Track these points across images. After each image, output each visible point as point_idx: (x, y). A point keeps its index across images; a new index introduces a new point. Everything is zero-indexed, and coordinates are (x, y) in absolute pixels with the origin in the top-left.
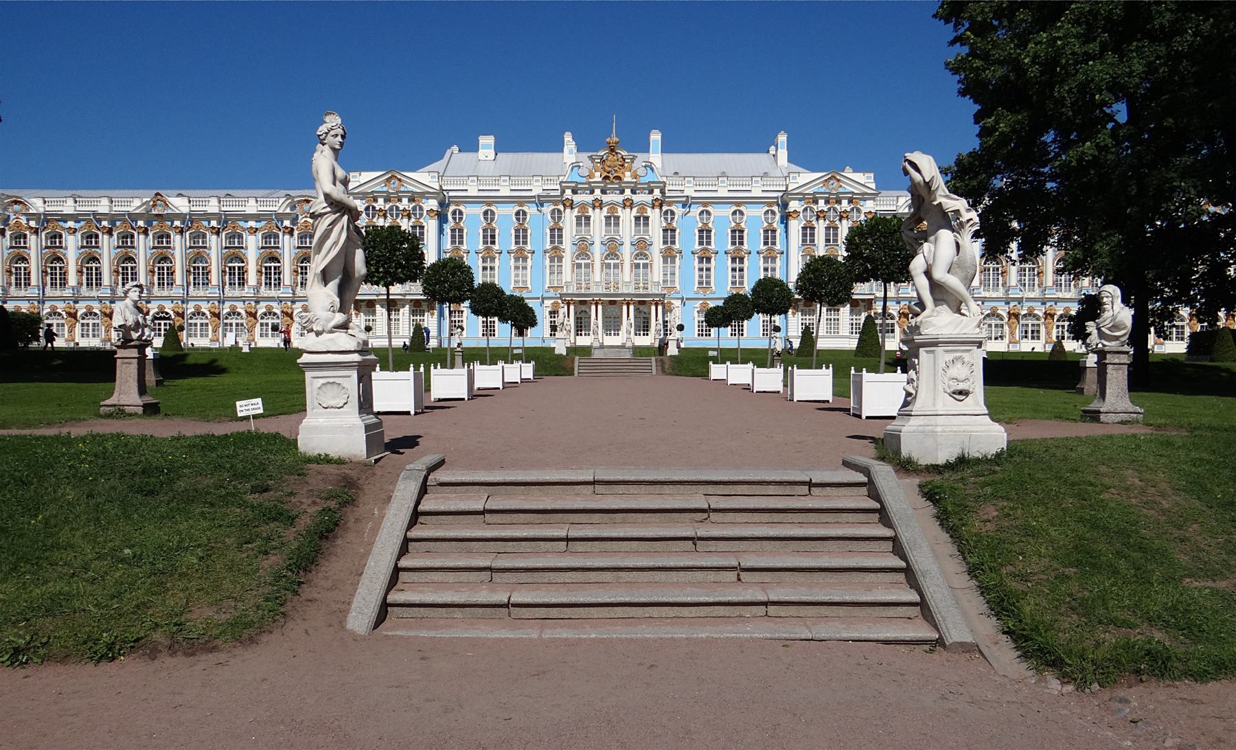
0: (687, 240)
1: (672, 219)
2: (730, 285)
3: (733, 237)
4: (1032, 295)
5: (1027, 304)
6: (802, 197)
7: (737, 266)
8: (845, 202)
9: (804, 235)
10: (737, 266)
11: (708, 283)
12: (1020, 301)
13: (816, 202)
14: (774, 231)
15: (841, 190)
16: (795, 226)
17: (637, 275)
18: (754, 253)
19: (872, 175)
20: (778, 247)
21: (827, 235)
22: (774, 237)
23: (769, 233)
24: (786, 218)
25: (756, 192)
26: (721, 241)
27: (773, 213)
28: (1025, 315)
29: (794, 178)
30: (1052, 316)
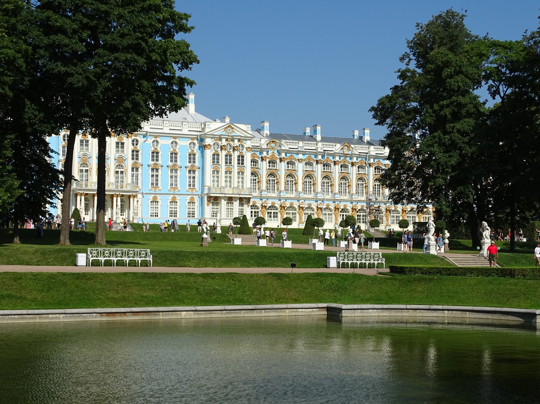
0: (145, 158)
1: (137, 144)
2: (188, 187)
3: (172, 157)
4: (328, 197)
5: (326, 203)
6: (213, 137)
7: (155, 173)
8: (236, 141)
9: (214, 159)
10: (174, 174)
11: (157, 184)
12: (323, 200)
13: (220, 139)
14: (194, 155)
15: (233, 134)
16: (209, 153)
17: (117, 178)
18: (183, 168)
19: (250, 126)
20: (198, 164)
21: (226, 159)
22: (194, 159)
23: (192, 156)
24: (203, 147)
25: (185, 131)
26: (164, 160)
27: (194, 144)
28: (325, 209)
29: (209, 125)
30: (338, 209)
